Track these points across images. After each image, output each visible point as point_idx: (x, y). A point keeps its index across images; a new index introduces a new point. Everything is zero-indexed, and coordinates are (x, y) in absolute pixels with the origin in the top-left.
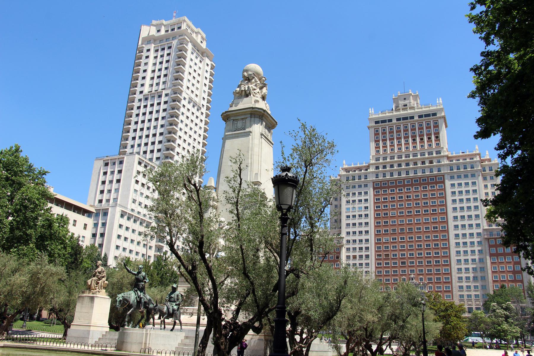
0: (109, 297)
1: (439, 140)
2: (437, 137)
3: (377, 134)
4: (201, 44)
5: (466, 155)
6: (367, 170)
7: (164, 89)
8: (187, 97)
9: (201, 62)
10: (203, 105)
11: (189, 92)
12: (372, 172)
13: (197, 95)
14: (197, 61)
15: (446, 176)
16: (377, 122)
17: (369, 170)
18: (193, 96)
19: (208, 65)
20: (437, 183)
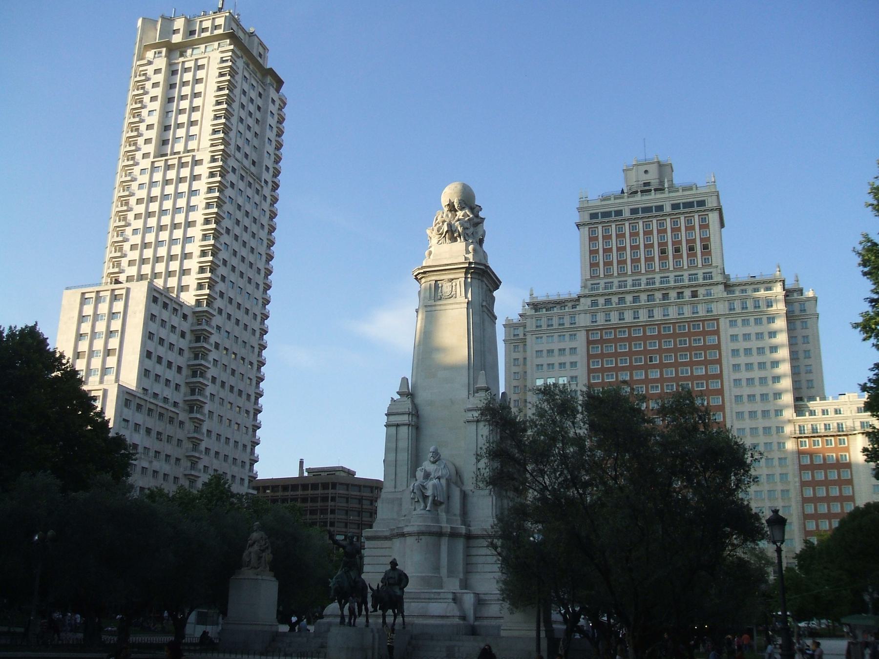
0: (274, 579)
1: (710, 253)
2: (705, 247)
3: (593, 239)
4: (259, 59)
5: (758, 283)
6: (574, 307)
7: (193, 150)
8: (236, 165)
9: (260, 95)
10: (266, 182)
11: (239, 156)
12: (585, 312)
13: (254, 163)
14: (253, 95)
15: (722, 321)
16: (593, 216)
17: (578, 308)
18: (247, 163)
19: (273, 101)
20: (705, 333)
